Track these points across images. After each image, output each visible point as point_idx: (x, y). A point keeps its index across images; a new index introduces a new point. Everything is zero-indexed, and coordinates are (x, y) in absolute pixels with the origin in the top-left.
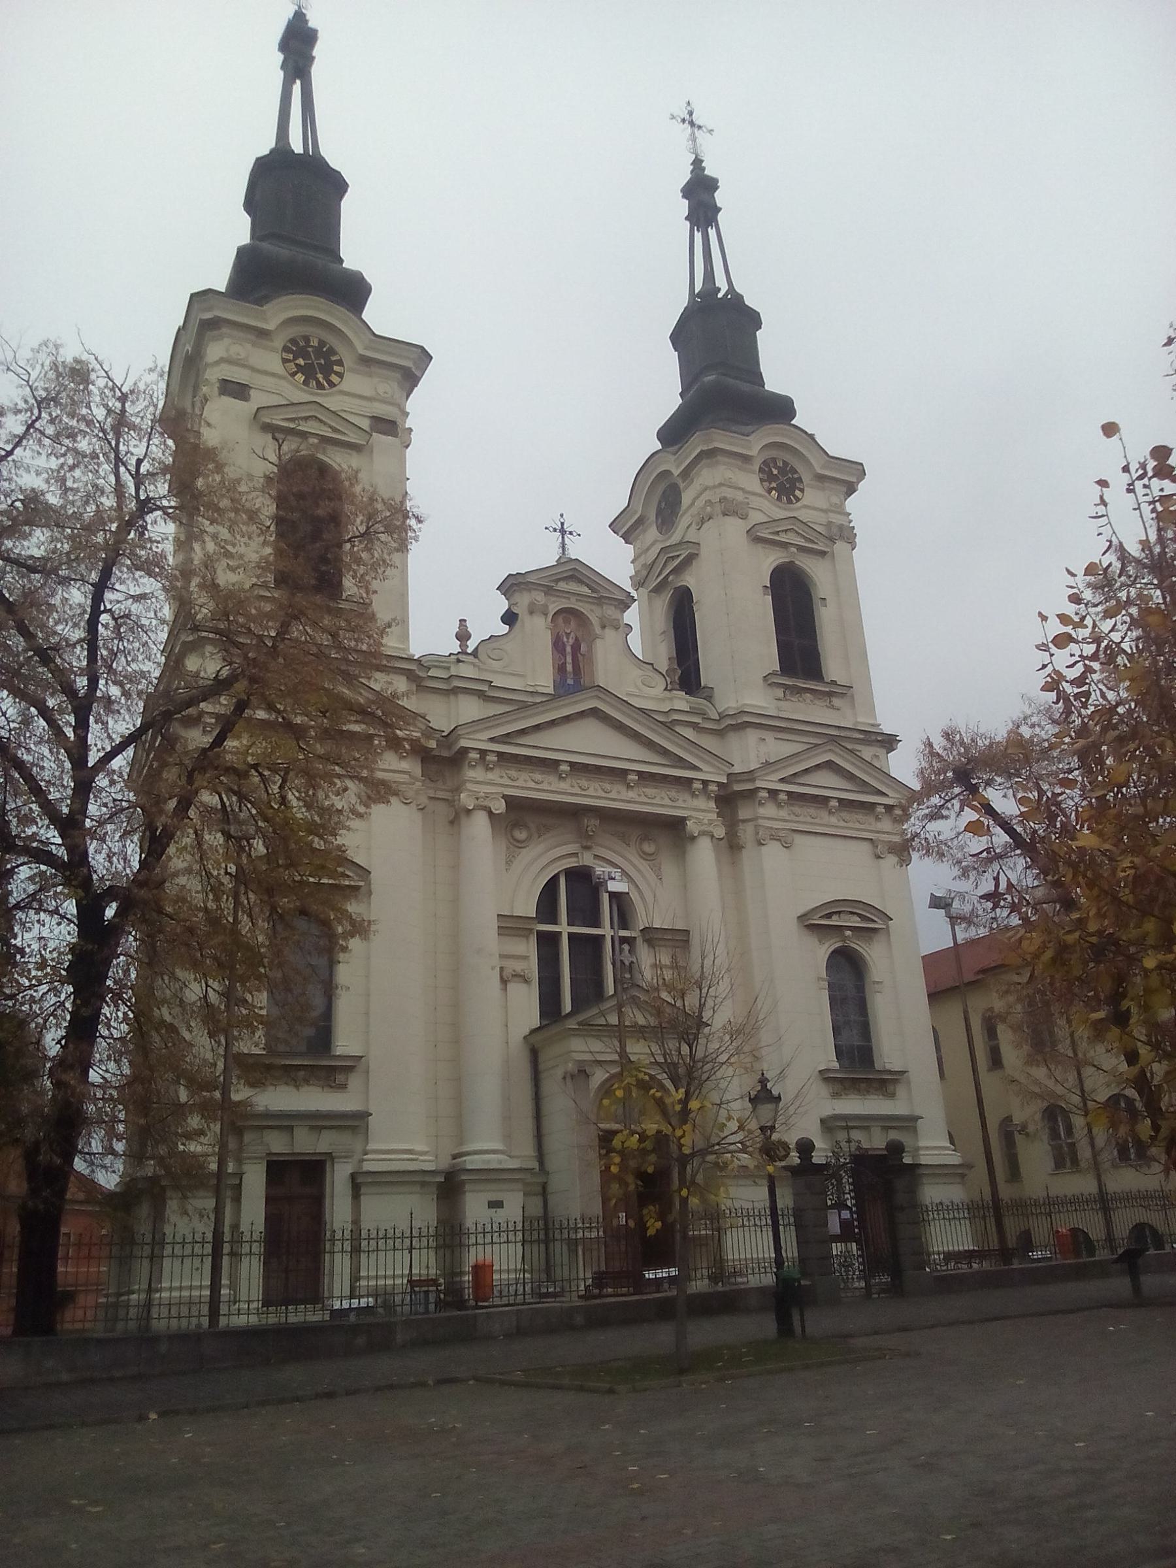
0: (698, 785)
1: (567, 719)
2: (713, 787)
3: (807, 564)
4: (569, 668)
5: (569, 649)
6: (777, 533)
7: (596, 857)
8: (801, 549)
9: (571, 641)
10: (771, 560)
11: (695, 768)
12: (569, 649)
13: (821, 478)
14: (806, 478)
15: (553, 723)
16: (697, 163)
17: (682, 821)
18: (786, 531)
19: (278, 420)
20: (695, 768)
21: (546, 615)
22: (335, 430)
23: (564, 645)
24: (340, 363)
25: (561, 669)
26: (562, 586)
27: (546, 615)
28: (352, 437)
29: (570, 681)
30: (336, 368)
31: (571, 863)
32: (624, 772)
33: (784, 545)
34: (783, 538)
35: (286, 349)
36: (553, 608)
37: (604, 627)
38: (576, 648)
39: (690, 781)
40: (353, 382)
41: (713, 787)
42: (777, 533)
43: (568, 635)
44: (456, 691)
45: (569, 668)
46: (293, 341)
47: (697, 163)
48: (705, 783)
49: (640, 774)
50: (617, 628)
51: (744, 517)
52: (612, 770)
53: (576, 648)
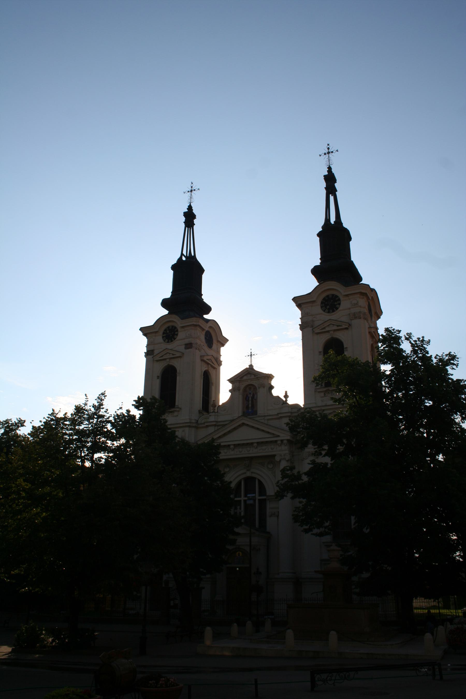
0: (279, 442)
1: (235, 429)
2: (285, 442)
3: (340, 336)
4: (250, 406)
5: (250, 399)
6: (324, 328)
7: (252, 473)
8: (335, 330)
9: (251, 395)
10: (324, 338)
11: (279, 436)
12: (250, 399)
13: (347, 295)
14: (341, 298)
15: (230, 432)
16: (330, 169)
17: (274, 456)
18: (329, 325)
19: (157, 358)
20: (279, 436)
21: (239, 390)
22: (173, 354)
23: (249, 398)
24: (177, 331)
25: (247, 407)
26: (245, 378)
27: (239, 390)
28: (178, 354)
29: (250, 410)
30: (176, 333)
31: (244, 476)
32: (252, 443)
33: (328, 332)
34: (327, 329)
35: (164, 333)
36: (242, 387)
37: (259, 388)
38: (253, 397)
39: (276, 441)
40: (181, 335)
41: (285, 442)
42: (324, 328)
43: (250, 394)
44: (207, 426)
45: (250, 406)
46: (165, 330)
47: (330, 169)
48: (282, 441)
49: (258, 443)
50: (264, 387)
51: (312, 327)
52: (247, 444)
53: (253, 397)
